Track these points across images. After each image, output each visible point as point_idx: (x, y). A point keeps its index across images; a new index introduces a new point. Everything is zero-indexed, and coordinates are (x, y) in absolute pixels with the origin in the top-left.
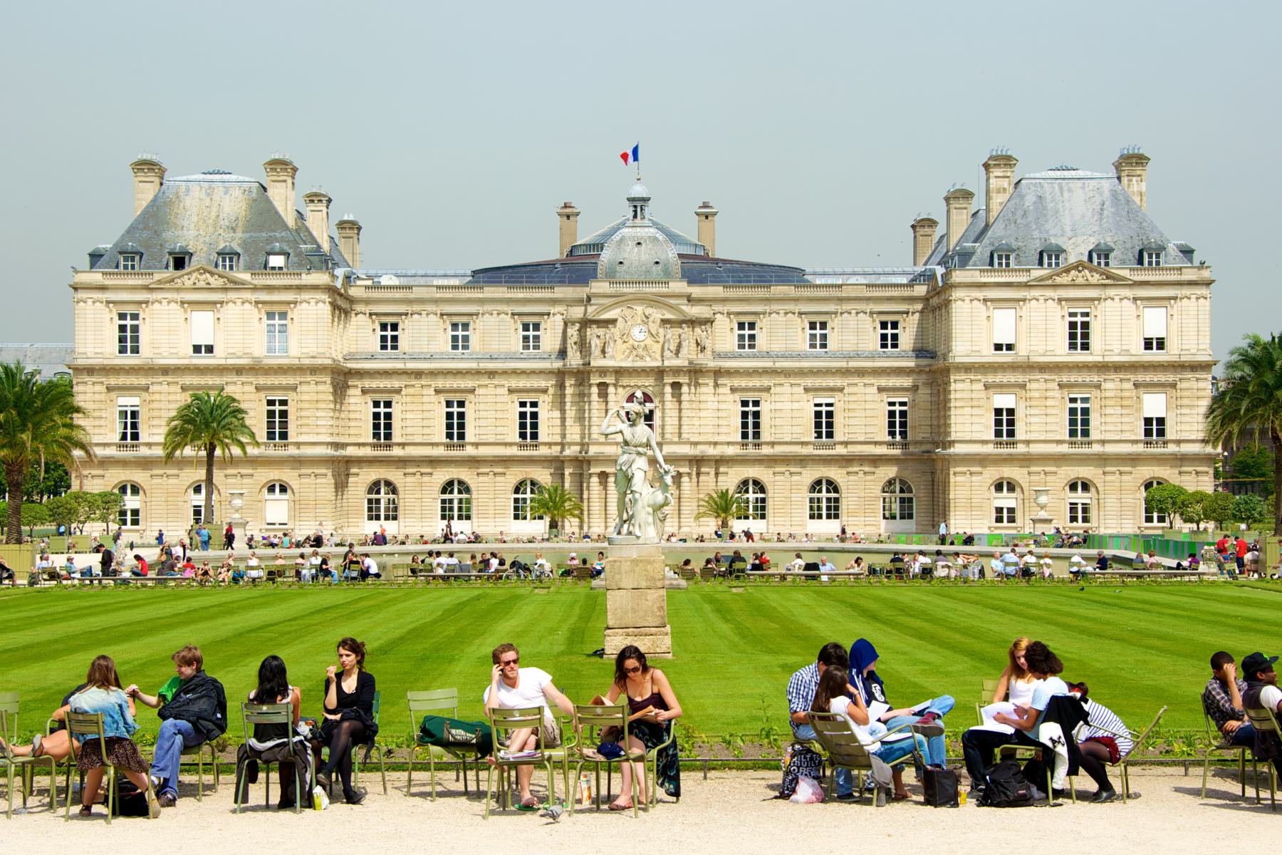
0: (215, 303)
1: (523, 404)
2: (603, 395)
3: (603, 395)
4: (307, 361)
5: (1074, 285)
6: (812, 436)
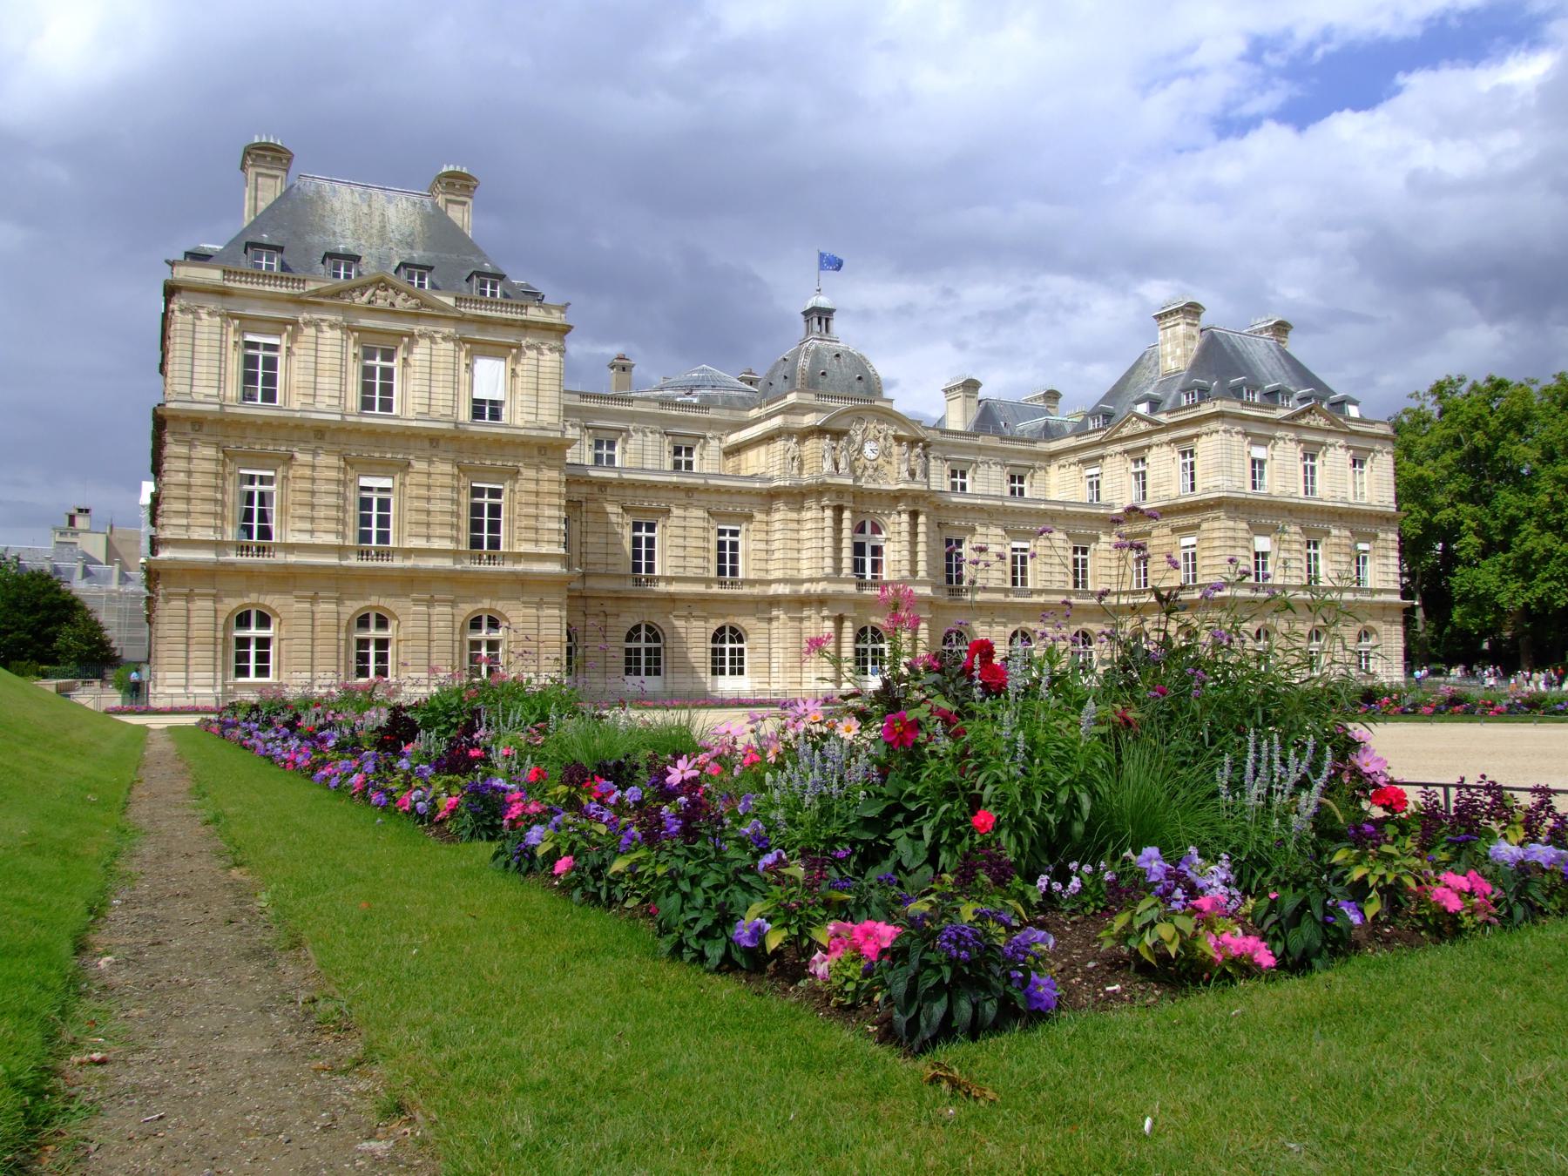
0: (401, 335)
1: (722, 532)
2: (838, 521)
3: (838, 521)
4: (534, 433)
5: (1308, 428)
6: (1009, 585)
